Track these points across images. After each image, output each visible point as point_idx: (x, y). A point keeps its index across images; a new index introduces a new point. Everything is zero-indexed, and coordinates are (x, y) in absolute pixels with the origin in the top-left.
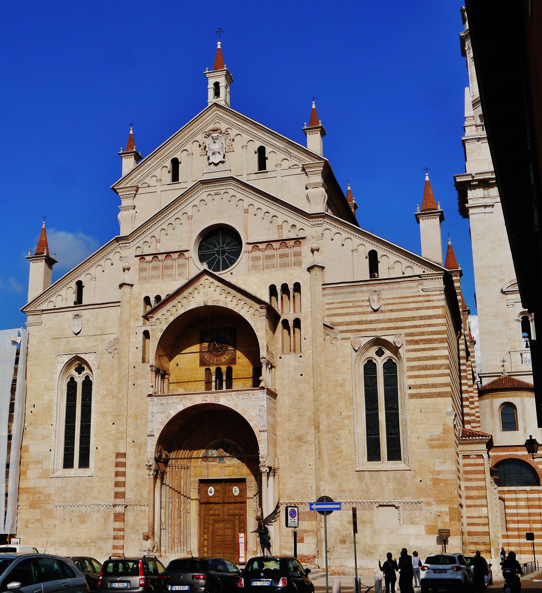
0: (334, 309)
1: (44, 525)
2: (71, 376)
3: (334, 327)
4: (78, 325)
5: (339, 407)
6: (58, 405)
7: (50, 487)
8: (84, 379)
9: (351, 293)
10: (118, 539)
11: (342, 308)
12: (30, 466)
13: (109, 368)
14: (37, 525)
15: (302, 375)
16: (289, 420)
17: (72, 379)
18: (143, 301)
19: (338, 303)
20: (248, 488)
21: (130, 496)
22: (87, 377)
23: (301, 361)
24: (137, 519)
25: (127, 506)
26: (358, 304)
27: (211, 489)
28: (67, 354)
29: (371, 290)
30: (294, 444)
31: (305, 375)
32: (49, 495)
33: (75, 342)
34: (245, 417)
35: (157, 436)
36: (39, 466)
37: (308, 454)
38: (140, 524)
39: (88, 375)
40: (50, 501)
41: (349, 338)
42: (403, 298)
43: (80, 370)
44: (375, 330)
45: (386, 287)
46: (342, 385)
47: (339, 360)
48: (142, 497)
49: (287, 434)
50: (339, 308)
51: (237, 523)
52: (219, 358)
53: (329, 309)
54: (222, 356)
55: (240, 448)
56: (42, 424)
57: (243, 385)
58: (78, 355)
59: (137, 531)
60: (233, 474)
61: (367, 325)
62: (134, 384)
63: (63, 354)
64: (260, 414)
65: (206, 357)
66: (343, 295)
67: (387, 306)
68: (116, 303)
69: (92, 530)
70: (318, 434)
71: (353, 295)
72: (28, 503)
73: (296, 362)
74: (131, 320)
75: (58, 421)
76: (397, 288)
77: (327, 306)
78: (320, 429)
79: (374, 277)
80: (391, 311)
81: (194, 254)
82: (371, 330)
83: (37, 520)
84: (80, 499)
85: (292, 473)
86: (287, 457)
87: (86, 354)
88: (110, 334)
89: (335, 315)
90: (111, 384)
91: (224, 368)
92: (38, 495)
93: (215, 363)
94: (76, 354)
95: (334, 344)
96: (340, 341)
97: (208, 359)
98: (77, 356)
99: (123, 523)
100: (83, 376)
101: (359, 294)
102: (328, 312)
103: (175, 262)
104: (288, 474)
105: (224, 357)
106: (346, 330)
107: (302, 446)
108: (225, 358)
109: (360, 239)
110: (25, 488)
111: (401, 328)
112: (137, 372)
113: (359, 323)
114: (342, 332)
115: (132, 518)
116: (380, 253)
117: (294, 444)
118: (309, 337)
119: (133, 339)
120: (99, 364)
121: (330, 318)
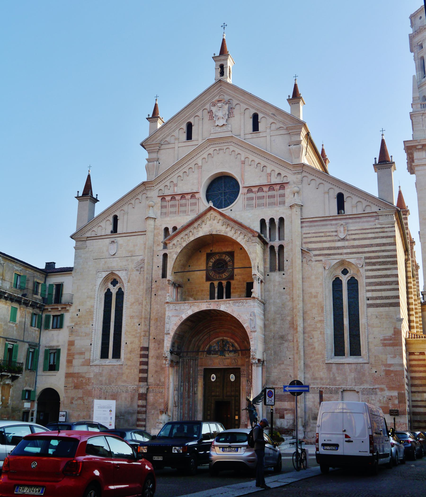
0: (310, 237)
1: (85, 402)
2: (107, 288)
4: (114, 249)
6: (98, 309)
7: (90, 372)
8: (117, 290)
9: (323, 225)
10: (141, 413)
11: (316, 237)
12: (76, 357)
14: (80, 401)
15: (284, 289)
16: (274, 324)
17: (109, 290)
18: (163, 231)
19: (313, 233)
20: (241, 376)
21: (151, 380)
22: (120, 289)
24: (156, 398)
26: (328, 234)
27: (213, 375)
30: (278, 342)
31: (287, 289)
32: (89, 379)
33: (111, 261)
34: (240, 320)
36: (82, 356)
37: (289, 350)
40: (90, 383)
41: (321, 261)
42: (363, 229)
43: (114, 282)
44: (341, 254)
45: (350, 221)
46: (315, 297)
47: (313, 277)
48: (160, 381)
49: (272, 334)
50: (313, 237)
51: (233, 402)
52: (221, 275)
53: (306, 238)
55: (236, 345)
56: (85, 324)
57: (239, 295)
58: (114, 272)
59: (156, 407)
60: (230, 364)
62: (155, 295)
64: (252, 318)
65: (211, 274)
66: (317, 227)
68: (143, 233)
70: (296, 334)
71: (324, 227)
72: (73, 385)
73: (280, 278)
74: (155, 246)
75: (97, 322)
76: (359, 222)
77: (304, 236)
78: (298, 330)
79: (341, 213)
80: (354, 239)
82: (338, 254)
83: (80, 398)
84: (113, 382)
86: (272, 352)
89: (311, 242)
90: (138, 294)
91: (224, 283)
92: (81, 379)
93: (218, 279)
95: (310, 265)
99: (145, 401)
101: (329, 227)
102: (305, 240)
103: (188, 200)
104: (272, 365)
106: (319, 254)
107: (284, 343)
110: (71, 373)
111: (364, 252)
113: (329, 248)
115: (152, 398)
117: (278, 342)
119: (155, 260)
120: (129, 279)
121: (306, 245)
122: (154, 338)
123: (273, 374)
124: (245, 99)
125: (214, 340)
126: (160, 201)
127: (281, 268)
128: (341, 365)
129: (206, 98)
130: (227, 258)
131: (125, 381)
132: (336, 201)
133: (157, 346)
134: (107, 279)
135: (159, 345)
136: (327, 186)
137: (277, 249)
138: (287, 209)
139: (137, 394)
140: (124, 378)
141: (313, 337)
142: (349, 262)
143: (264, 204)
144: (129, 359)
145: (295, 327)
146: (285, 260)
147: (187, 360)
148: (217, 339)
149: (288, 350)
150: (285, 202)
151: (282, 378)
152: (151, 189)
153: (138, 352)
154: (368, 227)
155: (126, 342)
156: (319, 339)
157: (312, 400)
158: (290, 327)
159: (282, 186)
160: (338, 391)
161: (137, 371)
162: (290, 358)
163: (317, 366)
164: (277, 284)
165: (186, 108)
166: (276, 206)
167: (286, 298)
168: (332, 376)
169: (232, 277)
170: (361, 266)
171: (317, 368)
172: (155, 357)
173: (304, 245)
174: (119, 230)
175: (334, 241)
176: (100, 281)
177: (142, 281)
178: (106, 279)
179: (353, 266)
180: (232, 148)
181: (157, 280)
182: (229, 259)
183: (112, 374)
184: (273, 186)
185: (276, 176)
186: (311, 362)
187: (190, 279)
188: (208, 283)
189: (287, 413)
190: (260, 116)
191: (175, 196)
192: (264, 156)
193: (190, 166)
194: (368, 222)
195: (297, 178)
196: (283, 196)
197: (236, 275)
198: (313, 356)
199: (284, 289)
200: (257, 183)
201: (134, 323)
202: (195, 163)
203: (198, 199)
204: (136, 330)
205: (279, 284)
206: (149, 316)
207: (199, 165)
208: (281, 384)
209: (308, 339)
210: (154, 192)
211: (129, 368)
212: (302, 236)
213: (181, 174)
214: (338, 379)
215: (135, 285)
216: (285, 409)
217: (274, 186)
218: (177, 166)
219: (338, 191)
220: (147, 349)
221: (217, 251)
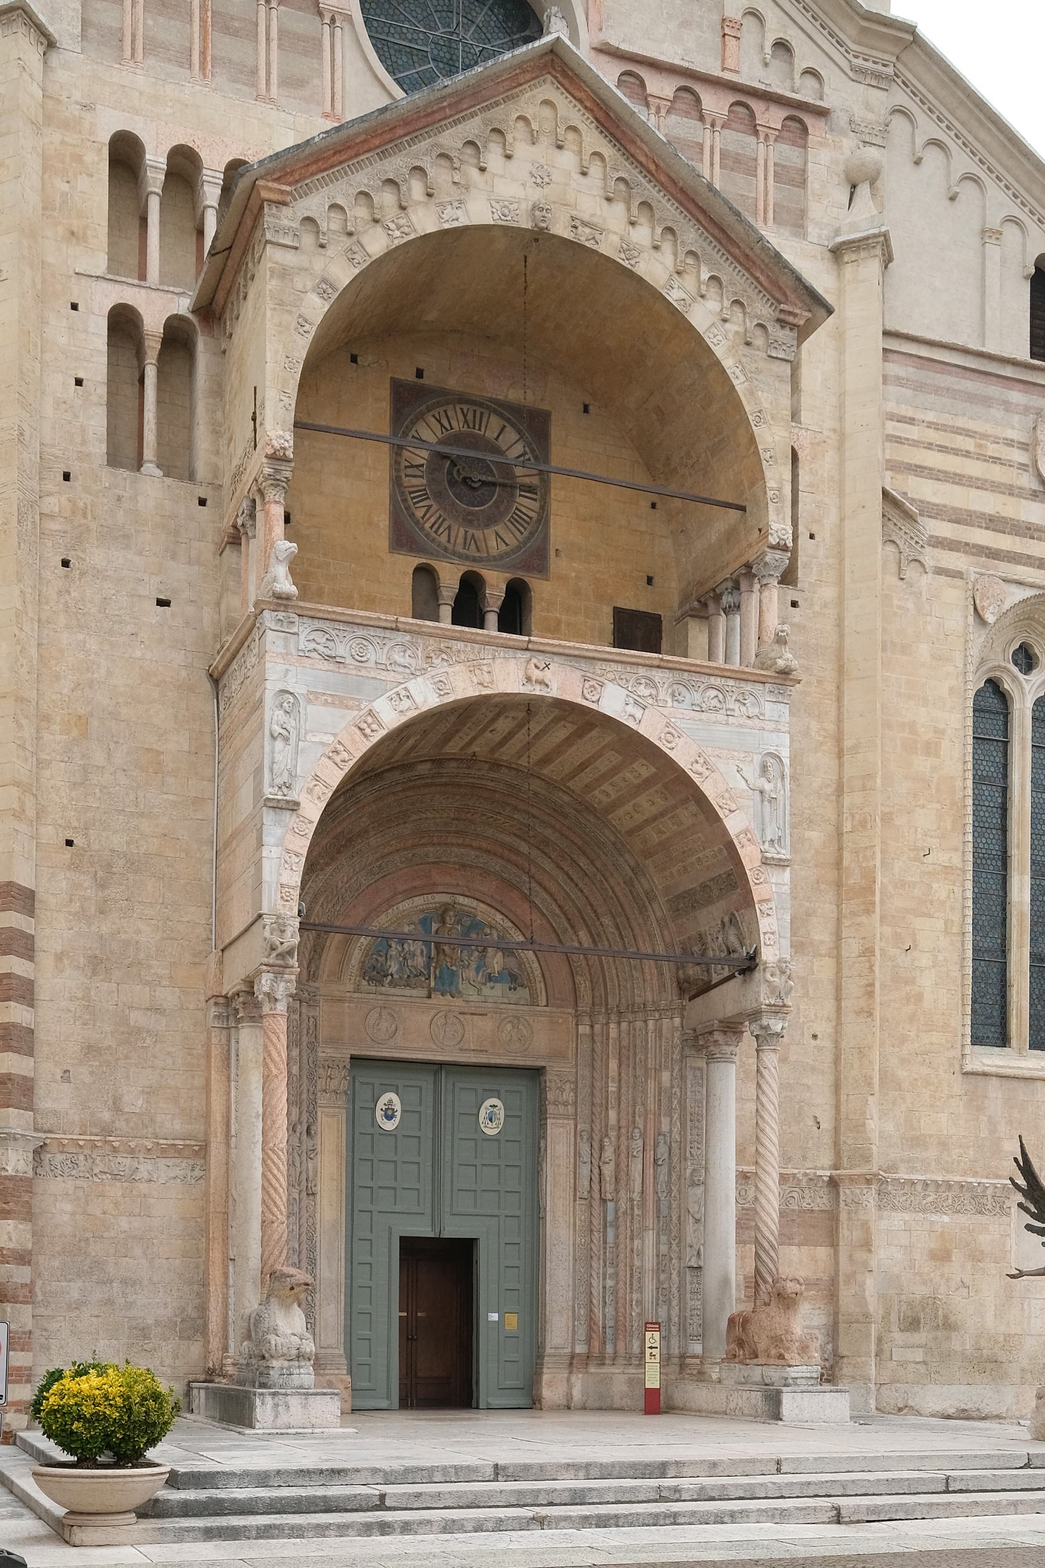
0: (915, 444)
3: (919, 519)
5: (916, 831)
9: (971, 398)
11: (943, 449)
19: (930, 425)
26: (992, 450)
35: (313, 810)
38: (106, 1235)
41: (958, 575)
46: (931, 749)
47: (923, 651)
48: (117, 1108)
50: (929, 446)
52: (478, 534)
54: (487, 526)
61: (1018, 539)
65: (419, 513)
77: (892, 427)
89: (918, 470)
93: (460, 549)
96: (930, 575)
97: (428, 525)
101: (997, 413)
105: (497, 534)
109: (1010, 193)
113: (995, 523)
114: (939, 543)
115: (68, 1207)
125: (406, 905)
138: (815, 257)
148: (419, 901)
150: (803, 213)
173: (889, 474)
175: (1016, 491)
182: (519, 449)
185: (768, 50)
195: (868, 107)
196: (798, 179)
209: (892, 951)
217: (757, 106)
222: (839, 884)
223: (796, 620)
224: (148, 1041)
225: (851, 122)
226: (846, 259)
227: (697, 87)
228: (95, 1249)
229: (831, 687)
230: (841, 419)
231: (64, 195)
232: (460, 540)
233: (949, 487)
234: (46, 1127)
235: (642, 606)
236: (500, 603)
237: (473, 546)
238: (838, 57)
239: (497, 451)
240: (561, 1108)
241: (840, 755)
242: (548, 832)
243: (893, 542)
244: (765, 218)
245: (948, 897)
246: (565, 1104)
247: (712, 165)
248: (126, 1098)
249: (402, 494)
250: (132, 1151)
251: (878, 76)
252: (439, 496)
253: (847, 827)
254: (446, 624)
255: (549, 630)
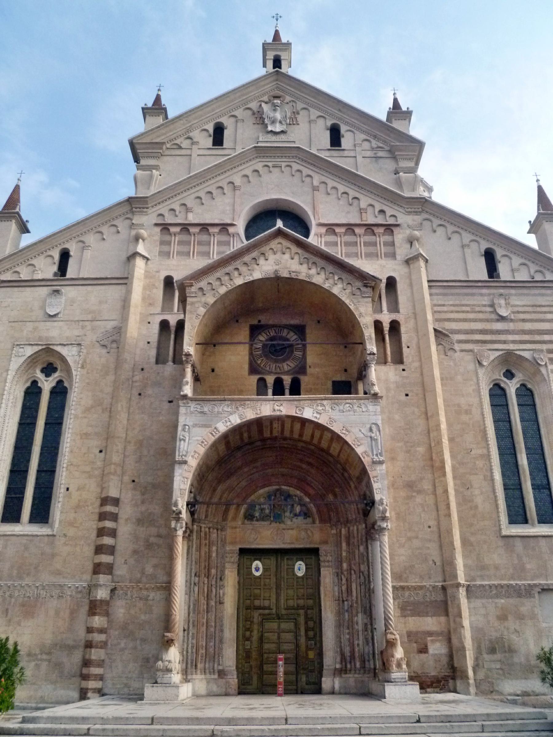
0: (446, 312)
2: (33, 379)
5: (466, 442)
6: (7, 418)
8: (53, 384)
9: (467, 295)
11: (457, 312)
13: (100, 368)
15: (407, 395)
21: (121, 571)
23: (405, 377)
25: (115, 588)
26: (477, 309)
28: (33, 343)
29: (494, 294)
33: (48, 328)
37: (426, 509)
39: (61, 378)
41: (471, 351)
44: (505, 342)
45: (513, 291)
46: (468, 412)
47: (459, 378)
48: (143, 572)
50: (452, 312)
52: (280, 365)
54: (284, 362)
58: (51, 347)
61: (493, 336)
62: (140, 394)
63: (25, 343)
65: (259, 362)
67: (516, 315)
69: (46, 630)
76: (528, 295)
77: (436, 309)
80: (524, 320)
81: (241, 228)
84: (28, 574)
85: (401, 539)
87: (65, 345)
88: (106, 320)
89: (449, 320)
90: (101, 391)
91: (287, 380)
94: (46, 345)
97: (262, 365)
98: (48, 348)
99: (106, 618)
100: (53, 380)
102: (438, 316)
105: (287, 364)
108: (287, 366)
112: (146, 377)
114: (460, 342)
115: (122, 611)
116: (499, 253)
118: (413, 345)
122: (134, 481)
123: (396, 558)
124: (318, 102)
126: (159, 232)
127: (399, 359)
128: (531, 539)
129: (251, 92)
130: (293, 337)
131: (58, 573)
132: (483, 260)
133: (139, 497)
134: (35, 361)
135: (143, 494)
136: (467, 237)
137: (386, 327)
139: (87, 601)
140: (58, 564)
141: (472, 487)
142: (520, 356)
143: (357, 253)
144: (71, 524)
145: (437, 464)
146: (404, 345)
147: (207, 530)
149: (424, 510)
151: (416, 566)
152: (143, 212)
153: (94, 508)
154: (543, 304)
155: (67, 486)
156: (484, 490)
157: (483, 611)
158: (424, 466)
159: (389, 229)
160: (533, 592)
161: (89, 551)
162: (429, 527)
163: (485, 542)
164: (392, 386)
165: (216, 99)
166: (380, 259)
167: (413, 413)
168: (516, 562)
169: (302, 369)
170: (544, 363)
171: (485, 547)
172: (134, 520)
174: (71, 272)
176: (16, 363)
177: (112, 366)
178: (31, 362)
179: (527, 364)
180: (295, 167)
181: (145, 366)
182: (295, 337)
183: (26, 554)
184: (373, 228)
185: (376, 213)
186: (472, 534)
187: (215, 370)
188: (254, 379)
189: (432, 641)
190: (343, 129)
191: (190, 228)
192: (353, 182)
193: (220, 184)
194: (543, 295)
196: (393, 244)
197: (310, 367)
198: (475, 522)
199: (407, 395)
200: (344, 222)
201: (89, 448)
202: (228, 180)
203: (233, 235)
204: (93, 462)
205: (397, 387)
206: (124, 435)
207: (235, 185)
208: (417, 580)
209: (461, 490)
210: (147, 217)
211: (71, 543)
212: (432, 309)
213: (202, 194)
214: (528, 566)
215: (97, 373)
216: (428, 632)
218: (196, 180)
219: (485, 245)
220: (116, 502)
221: (271, 322)
222: (432, 466)
223: (405, 375)
224: (156, 547)
225: (408, 226)
226: (410, 263)
227: (353, 227)
228: (131, 627)
229: (421, 396)
230: (415, 309)
231: (149, 295)
232: (274, 368)
233: (461, 323)
234: (117, 581)
235: (343, 379)
236: (289, 385)
237: (278, 369)
238: (401, 210)
239: (288, 340)
240: (327, 564)
241: (427, 419)
242: (310, 460)
243: (441, 344)
244: (381, 258)
245: (484, 466)
246: (328, 561)
247: (360, 246)
248: (147, 569)
249: (253, 357)
250: (147, 589)
251: (416, 212)
252: (266, 356)
253: (433, 445)
254: (270, 396)
255: (307, 391)
